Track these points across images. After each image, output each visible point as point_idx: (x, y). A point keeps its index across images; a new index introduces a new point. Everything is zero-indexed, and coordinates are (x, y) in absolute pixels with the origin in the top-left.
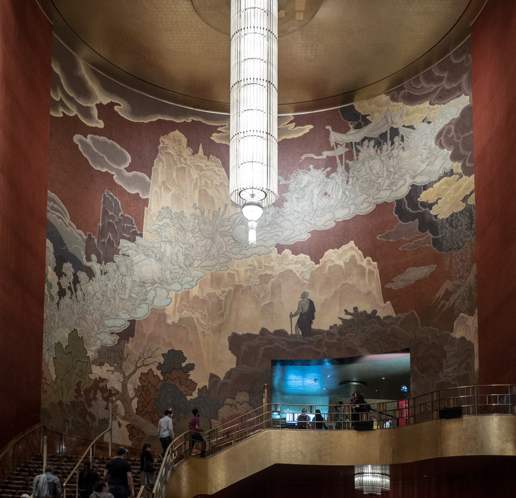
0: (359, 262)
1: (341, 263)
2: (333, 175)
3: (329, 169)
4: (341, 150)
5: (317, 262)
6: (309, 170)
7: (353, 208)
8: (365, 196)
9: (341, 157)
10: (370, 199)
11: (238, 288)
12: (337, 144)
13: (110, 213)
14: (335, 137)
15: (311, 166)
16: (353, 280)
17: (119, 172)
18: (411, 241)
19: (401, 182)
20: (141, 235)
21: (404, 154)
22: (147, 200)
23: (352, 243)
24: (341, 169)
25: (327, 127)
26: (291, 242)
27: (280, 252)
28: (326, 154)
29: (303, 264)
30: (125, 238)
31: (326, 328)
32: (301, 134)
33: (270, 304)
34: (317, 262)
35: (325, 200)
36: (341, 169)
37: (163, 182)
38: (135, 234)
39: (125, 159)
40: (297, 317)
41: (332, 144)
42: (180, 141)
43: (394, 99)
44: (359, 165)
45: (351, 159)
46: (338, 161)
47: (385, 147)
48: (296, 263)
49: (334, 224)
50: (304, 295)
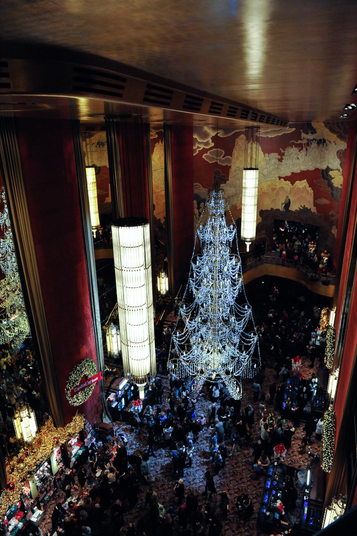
0: (307, 189)
1: (301, 187)
2: (301, 151)
3: (300, 148)
4: (305, 142)
5: (293, 185)
6: (293, 147)
7: (307, 166)
8: (312, 163)
9: (305, 144)
10: (313, 165)
11: (264, 193)
12: (304, 138)
13: (216, 176)
14: (303, 135)
15: (294, 146)
16: (304, 195)
17: (220, 160)
18: (325, 188)
19: (324, 163)
20: (228, 180)
21: (327, 152)
22: (231, 166)
23: (305, 180)
24: (304, 149)
25: (301, 130)
26: (284, 176)
27: (279, 180)
28: (300, 142)
29: (288, 185)
30: (222, 183)
31: (294, 210)
32: (291, 132)
33: (275, 199)
34: (293, 185)
35: (297, 161)
36: (304, 149)
37: (237, 157)
38: (226, 180)
39: (221, 153)
40: (284, 205)
41: (302, 138)
42: (243, 139)
43: (326, 126)
44: (311, 149)
45: (308, 146)
46: (304, 146)
47: (321, 145)
48: (285, 184)
49: (300, 171)
50: (287, 197)
